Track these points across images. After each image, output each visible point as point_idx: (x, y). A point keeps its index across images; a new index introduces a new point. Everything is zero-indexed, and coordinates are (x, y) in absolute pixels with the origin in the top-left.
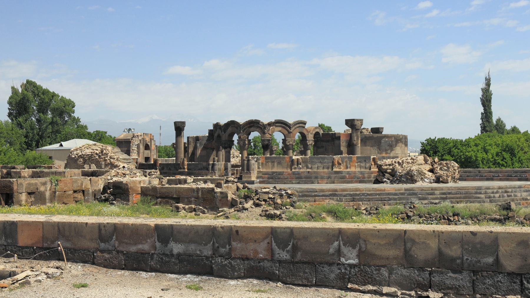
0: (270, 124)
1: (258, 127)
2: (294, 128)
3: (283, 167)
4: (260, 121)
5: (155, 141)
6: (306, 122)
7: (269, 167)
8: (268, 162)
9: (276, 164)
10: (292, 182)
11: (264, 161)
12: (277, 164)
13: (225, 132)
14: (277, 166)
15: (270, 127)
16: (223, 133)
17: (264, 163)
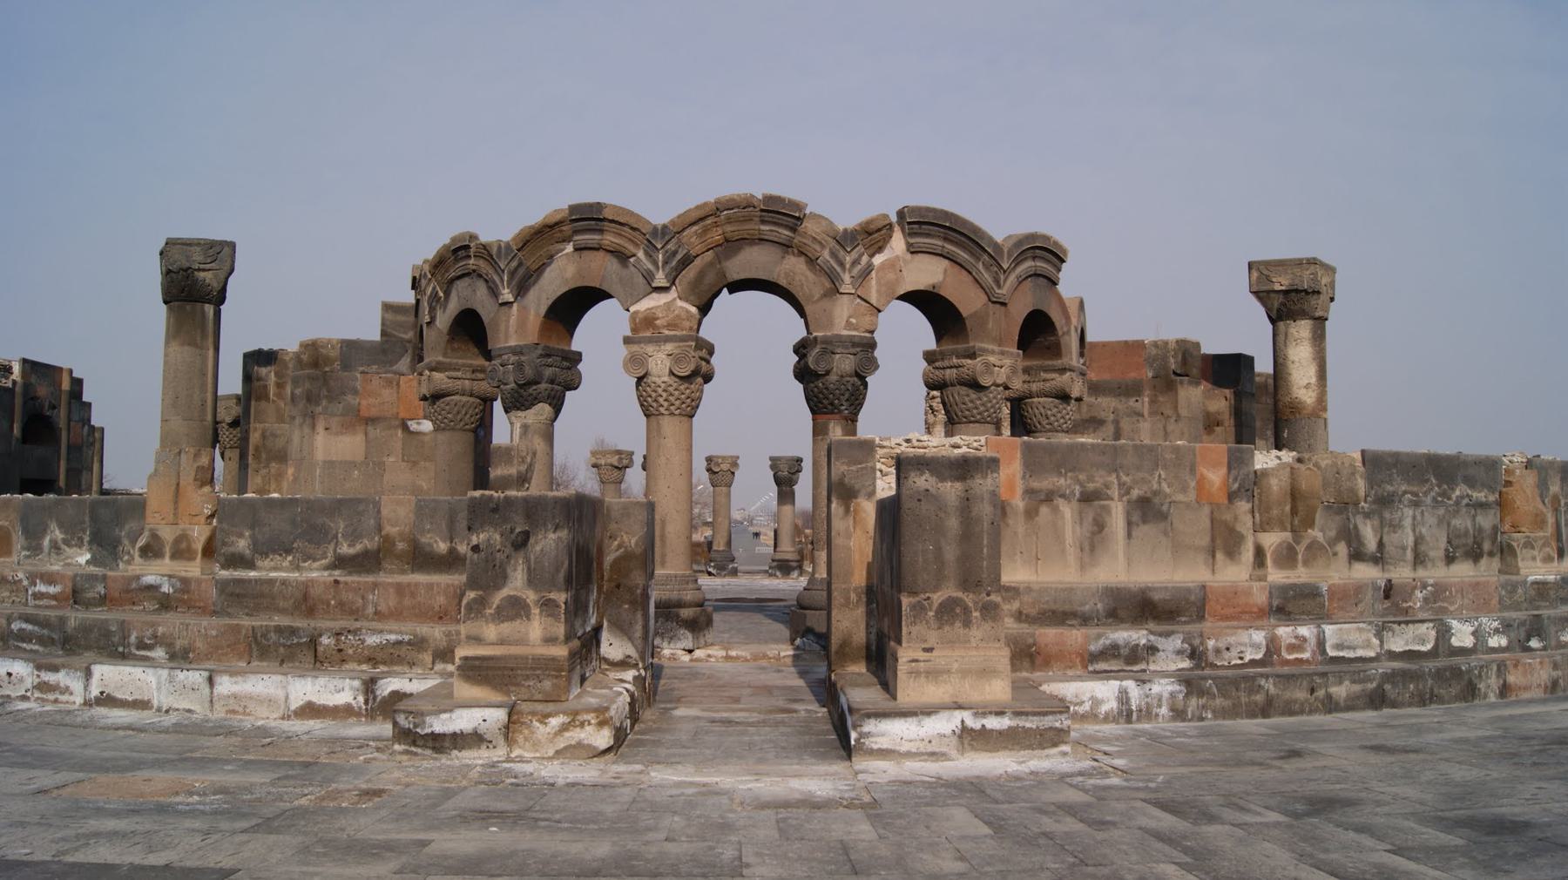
0: (872, 235)
1: (786, 246)
2: (1012, 278)
3: (1179, 549)
4: (798, 206)
5: (89, 405)
6: (1065, 252)
7: (1059, 537)
8: (1049, 497)
9: (1117, 514)
10: (1329, 697)
11: (1019, 489)
12: (1128, 514)
13: (521, 290)
14: (1129, 535)
15: (872, 256)
16: (507, 295)
17: (1019, 503)
